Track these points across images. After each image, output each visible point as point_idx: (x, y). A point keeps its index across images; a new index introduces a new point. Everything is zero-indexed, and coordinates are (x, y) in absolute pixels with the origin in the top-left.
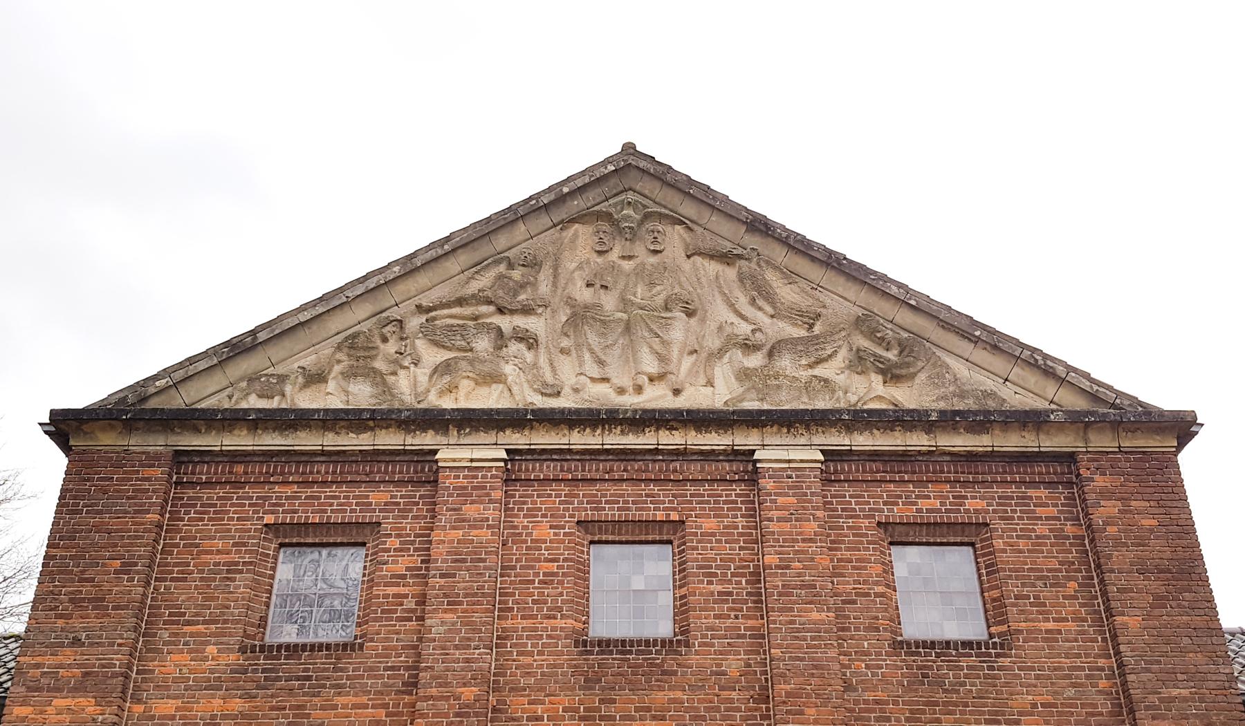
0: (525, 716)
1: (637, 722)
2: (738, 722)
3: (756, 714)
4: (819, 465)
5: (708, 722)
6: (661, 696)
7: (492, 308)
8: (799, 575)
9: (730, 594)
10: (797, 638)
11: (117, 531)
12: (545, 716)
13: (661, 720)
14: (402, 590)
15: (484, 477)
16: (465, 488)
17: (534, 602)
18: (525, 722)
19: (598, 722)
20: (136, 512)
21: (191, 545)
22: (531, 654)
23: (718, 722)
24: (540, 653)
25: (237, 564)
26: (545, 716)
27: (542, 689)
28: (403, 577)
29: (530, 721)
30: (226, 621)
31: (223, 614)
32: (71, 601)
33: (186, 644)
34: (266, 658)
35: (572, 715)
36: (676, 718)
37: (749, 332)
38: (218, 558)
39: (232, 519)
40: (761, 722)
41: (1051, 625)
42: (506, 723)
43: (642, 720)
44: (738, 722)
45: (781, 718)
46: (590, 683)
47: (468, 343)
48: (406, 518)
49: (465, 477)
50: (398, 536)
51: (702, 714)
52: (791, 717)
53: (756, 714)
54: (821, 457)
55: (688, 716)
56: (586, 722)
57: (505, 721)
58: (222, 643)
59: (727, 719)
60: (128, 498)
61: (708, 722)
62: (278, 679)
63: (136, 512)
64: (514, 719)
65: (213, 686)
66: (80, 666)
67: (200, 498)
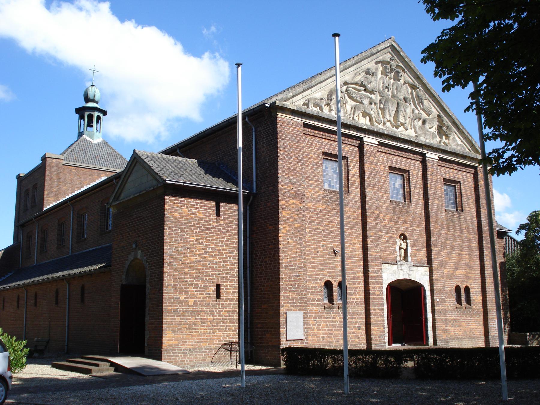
4: (437, 161)
6: (407, 218)
7: (364, 89)
8: (434, 191)
9: (418, 193)
10: (433, 207)
11: (295, 148)
14: (355, 179)
15: (373, 149)
16: (369, 152)
17: (382, 188)
20: (298, 142)
21: (307, 155)
22: (382, 203)
24: (384, 203)
25: (318, 163)
27: (385, 213)
28: (354, 175)
30: (319, 181)
31: (318, 179)
32: (288, 169)
33: (311, 187)
34: (329, 194)
37: (417, 113)
38: (314, 160)
39: (315, 148)
41: (469, 209)
46: (394, 212)
47: (361, 100)
48: (353, 157)
49: (370, 148)
50: (352, 162)
54: (438, 159)
58: (319, 188)
60: (295, 137)
62: (332, 201)
63: (298, 142)
65: (319, 200)
66: (294, 191)
67: (306, 139)
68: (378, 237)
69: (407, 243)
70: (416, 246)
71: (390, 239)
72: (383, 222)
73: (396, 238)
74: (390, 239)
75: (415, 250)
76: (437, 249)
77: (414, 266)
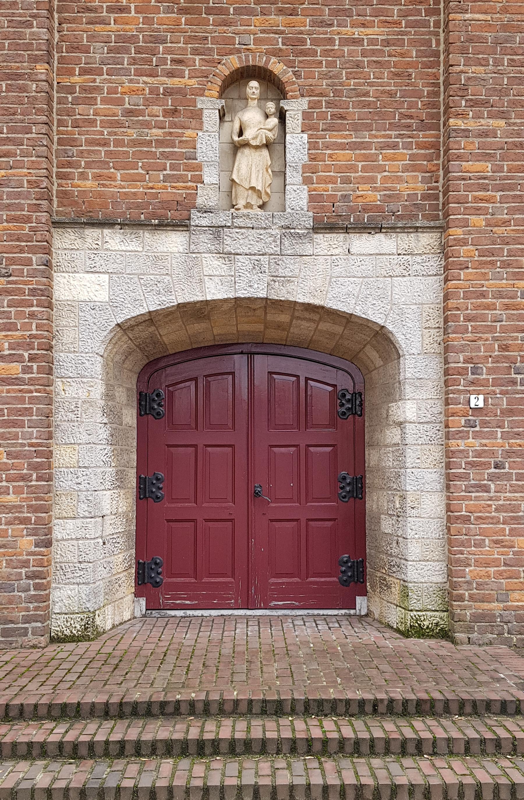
0: (105, 5)
1: (258, 17)
2: (395, 18)
3: (420, 7)
5: (355, 18)
12: (132, 6)
13: (291, 15)
18: (105, 14)
19: (204, 15)
23: (368, 18)
26: (132, 6)
29: (113, 12)
35: (168, 6)
36: (311, 12)
40: (426, 18)
42: (79, 14)
43: (265, 14)
44: (395, 18)
45: (457, 6)
51: (347, 7)
52: (470, 4)
53: (420, 7)
55: (327, 10)
56: (188, 16)
57: (78, 12)
59: (381, 14)
61: (355, 18)
64: (89, 10)
68: (23, 89)
69: (282, 116)
70: (356, 128)
71: (148, 103)
72: (105, 22)
73: (201, 93)
74: (148, 103)
75: (342, 147)
76: (502, 123)
77: (316, 229)
